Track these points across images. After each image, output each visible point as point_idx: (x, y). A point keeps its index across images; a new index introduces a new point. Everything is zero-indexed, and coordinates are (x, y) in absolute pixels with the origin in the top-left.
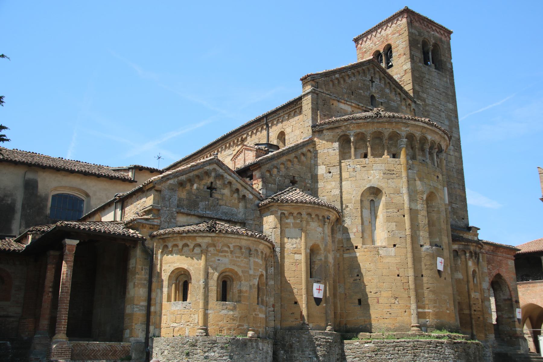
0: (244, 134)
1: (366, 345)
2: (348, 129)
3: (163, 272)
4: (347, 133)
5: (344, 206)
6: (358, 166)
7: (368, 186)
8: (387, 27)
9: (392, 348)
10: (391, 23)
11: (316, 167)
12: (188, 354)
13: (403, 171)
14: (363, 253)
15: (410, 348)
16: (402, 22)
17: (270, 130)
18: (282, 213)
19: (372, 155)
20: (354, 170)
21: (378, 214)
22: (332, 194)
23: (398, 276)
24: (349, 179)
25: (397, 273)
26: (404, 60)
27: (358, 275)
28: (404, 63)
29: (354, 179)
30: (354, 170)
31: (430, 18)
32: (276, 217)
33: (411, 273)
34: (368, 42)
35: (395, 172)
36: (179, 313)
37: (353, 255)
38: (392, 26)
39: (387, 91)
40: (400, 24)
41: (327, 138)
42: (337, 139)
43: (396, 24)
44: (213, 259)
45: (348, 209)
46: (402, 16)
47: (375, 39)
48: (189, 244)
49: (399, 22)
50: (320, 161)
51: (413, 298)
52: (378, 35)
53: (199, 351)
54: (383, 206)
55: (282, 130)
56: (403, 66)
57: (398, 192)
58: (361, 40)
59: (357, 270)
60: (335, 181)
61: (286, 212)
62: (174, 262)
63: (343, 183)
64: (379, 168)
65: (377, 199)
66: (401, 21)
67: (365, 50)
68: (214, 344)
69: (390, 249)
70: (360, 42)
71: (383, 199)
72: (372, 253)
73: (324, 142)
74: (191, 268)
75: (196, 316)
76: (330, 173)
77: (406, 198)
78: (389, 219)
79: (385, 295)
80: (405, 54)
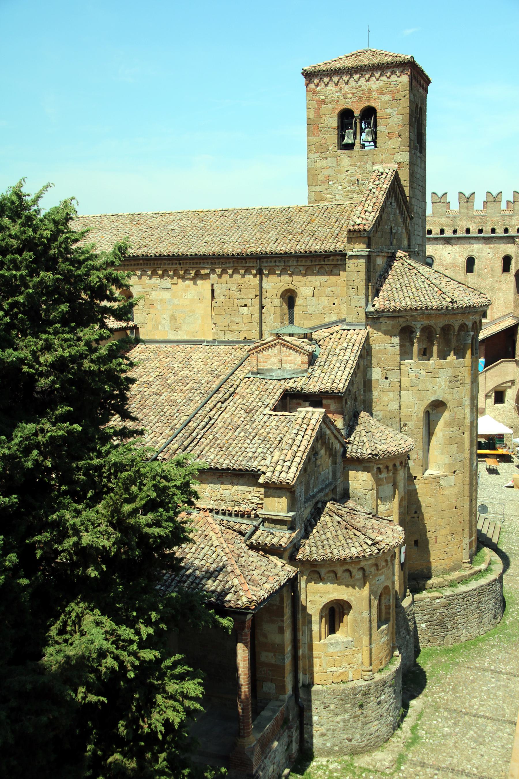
0: (207, 268)
1: (438, 601)
2: (415, 320)
3: (308, 603)
4: (412, 325)
5: (402, 423)
6: (422, 372)
7: (432, 399)
8: (371, 76)
9: (461, 600)
10: (379, 73)
11: (369, 369)
12: (361, 706)
13: (467, 375)
14: (424, 485)
15: (476, 596)
16: (400, 79)
17: (264, 278)
18: (379, 468)
19: (438, 356)
20: (417, 377)
21: (436, 430)
22: (390, 408)
23: (456, 508)
24: (410, 388)
25: (455, 504)
26: (398, 145)
27: (416, 512)
28: (398, 150)
29: (416, 388)
30: (417, 377)
31: (426, 72)
32: (372, 475)
33: (468, 503)
34: (331, 87)
35: (459, 378)
36: (339, 654)
37: (412, 488)
38: (381, 78)
39: (398, 212)
40: (396, 81)
41: (384, 328)
42: (398, 331)
43: (389, 78)
44: (374, 582)
45: (406, 428)
46: (401, 69)
47: (346, 89)
48: (351, 570)
49: (394, 78)
50: (374, 361)
51: (467, 531)
52: (352, 83)
53: (372, 699)
54: (445, 422)
55: (291, 287)
56: (396, 155)
57: (460, 404)
58: (319, 77)
59: (415, 506)
60: (393, 391)
61: (381, 466)
62: (328, 593)
63: (403, 393)
64: (446, 374)
65: (435, 411)
66: (399, 77)
67: (324, 97)
68: (384, 685)
69: (451, 477)
70: (316, 81)
71: (446, 415)
72: (433, 485)
73: (380, 334)
74: (352, 599)
75: (360, 655)
76: (386, 378)
77: (468, 411)
78: (451, 440)
79: (444, 531)
80: (400, 136)
